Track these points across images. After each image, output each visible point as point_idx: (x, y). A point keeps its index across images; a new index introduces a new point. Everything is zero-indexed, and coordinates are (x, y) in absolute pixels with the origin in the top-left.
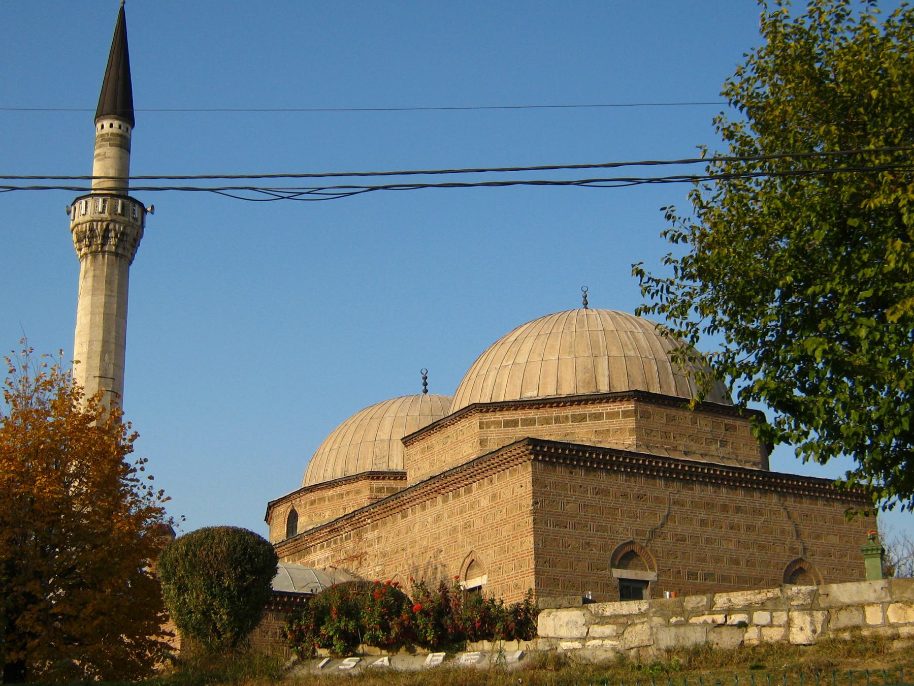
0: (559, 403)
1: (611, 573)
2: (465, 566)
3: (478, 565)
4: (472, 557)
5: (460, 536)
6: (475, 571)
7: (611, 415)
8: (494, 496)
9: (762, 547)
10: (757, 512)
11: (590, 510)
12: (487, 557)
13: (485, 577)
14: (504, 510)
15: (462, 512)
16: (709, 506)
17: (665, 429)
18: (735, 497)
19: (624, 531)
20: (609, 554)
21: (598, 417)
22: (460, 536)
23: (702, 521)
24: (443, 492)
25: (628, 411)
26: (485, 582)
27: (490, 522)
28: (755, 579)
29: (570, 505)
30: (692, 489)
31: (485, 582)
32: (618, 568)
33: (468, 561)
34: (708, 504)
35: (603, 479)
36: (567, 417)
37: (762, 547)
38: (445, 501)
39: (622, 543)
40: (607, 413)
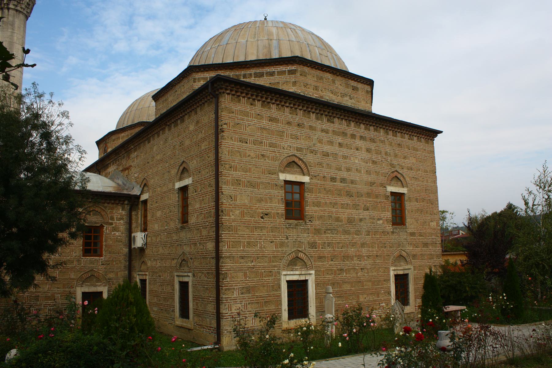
0: (246, 65)
1: (278, 175)
2: (180, 171)
3: (187, 171)
4: (184, 165)
5: (177, 152)
6: (186, 174)
7: (281, 73)
8: (198, 122)
9: (374, 162)
10: (373, 140)
11: (265, 132)
12: (193, 165)
13: (191, 178)
14: (203, 131)
15: (179, 136)
16: (344, 134)
17: (316, 84)
18: (359, 130)
19: (288, 146)
20: (277, 163)
21: (272, 74)
22: (177, 152)
23: (339, 143)
24: (168, 124)
25: (291, 70)
26: (191, 182)
27: (195, 140)
28: (371, 183)
29: (250, 127)
30: (333, 123)
31: (191, 182)
32: (283, 172)
33: (181, 168)
34: (343, 133)
35: (274, 111)
36: (251, 75)
37: (374, 162)
38: (169, 130)
39: (287, 155)
40: (278, 72)
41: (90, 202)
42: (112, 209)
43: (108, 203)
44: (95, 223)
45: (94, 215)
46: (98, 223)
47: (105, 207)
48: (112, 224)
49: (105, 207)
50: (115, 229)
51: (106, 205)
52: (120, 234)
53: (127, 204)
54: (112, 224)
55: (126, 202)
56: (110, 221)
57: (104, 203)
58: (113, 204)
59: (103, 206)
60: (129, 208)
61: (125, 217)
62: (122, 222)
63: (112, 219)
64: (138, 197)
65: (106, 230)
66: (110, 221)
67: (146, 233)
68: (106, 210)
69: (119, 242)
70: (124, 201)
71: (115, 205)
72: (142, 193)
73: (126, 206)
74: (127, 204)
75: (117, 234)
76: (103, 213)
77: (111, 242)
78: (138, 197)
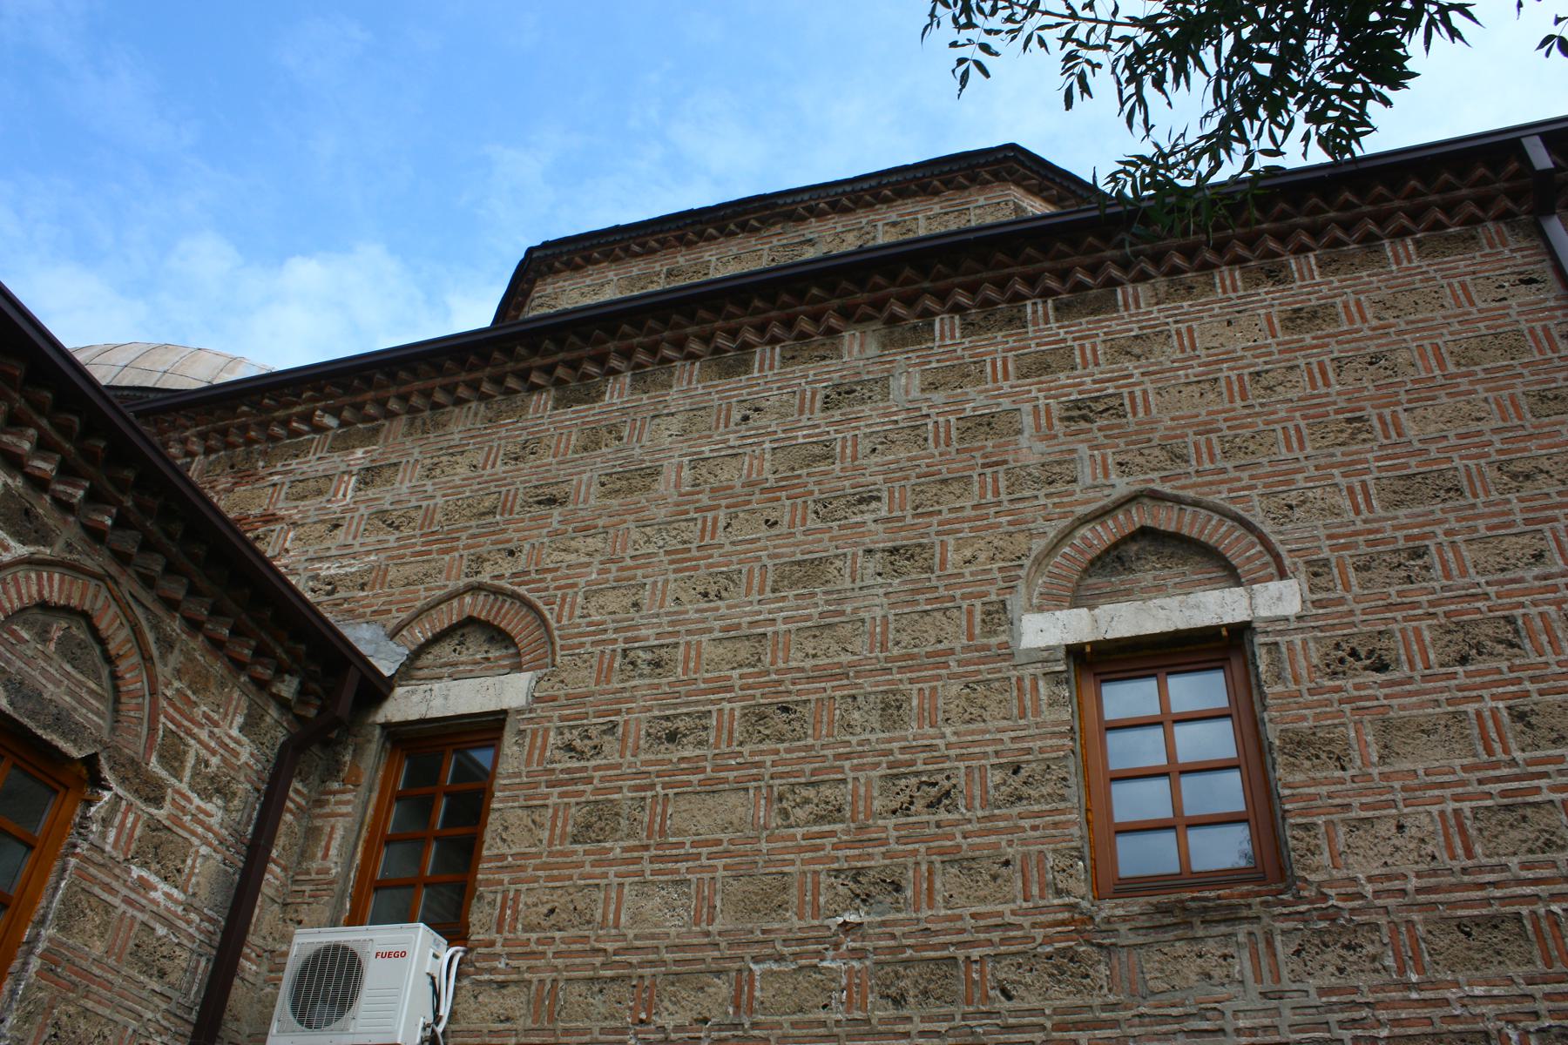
31: (1292, 606)
41: (95, 535)
42: (200, 683)
43: (194, 626)
44: (61, 721)
45: (68, 650)
46: (73, 731)
47: (167, 644)
48: (157, 801)
49: (167, 644)
50: (159, 847)
51: (175, 626)
52: (173, 901)
53: (283, 704)
54: (153, 793)
55: (288, 688)
56: (154, 765)
57: (171, 605)
58: (216, 645)
59: (155, 627)
60: (281, 736)
61: (242, 787)
62: (214, 808)
63: (173, 757)
64: (376, 689)
65: (112, 817)
66: (154, 765)
67: (458, 950)
68: (159, 667)
69: (147, 968)
70: (280, 671)
71: (218, 668)
72: (407, 671)
73: (273, 713)
74: (283, 704)
75: (161, 891)
76: (134, 680)
77: (98, 948)
78: (376, 689)
